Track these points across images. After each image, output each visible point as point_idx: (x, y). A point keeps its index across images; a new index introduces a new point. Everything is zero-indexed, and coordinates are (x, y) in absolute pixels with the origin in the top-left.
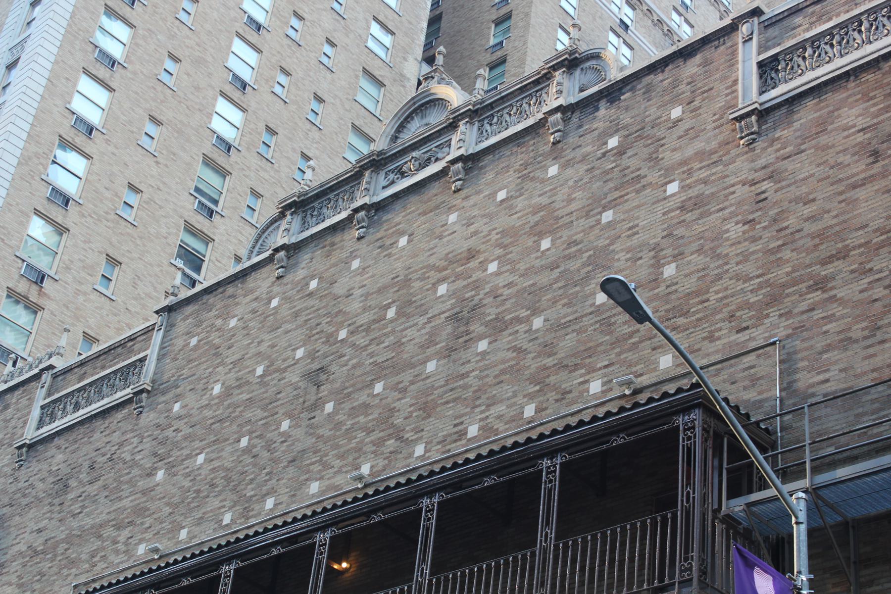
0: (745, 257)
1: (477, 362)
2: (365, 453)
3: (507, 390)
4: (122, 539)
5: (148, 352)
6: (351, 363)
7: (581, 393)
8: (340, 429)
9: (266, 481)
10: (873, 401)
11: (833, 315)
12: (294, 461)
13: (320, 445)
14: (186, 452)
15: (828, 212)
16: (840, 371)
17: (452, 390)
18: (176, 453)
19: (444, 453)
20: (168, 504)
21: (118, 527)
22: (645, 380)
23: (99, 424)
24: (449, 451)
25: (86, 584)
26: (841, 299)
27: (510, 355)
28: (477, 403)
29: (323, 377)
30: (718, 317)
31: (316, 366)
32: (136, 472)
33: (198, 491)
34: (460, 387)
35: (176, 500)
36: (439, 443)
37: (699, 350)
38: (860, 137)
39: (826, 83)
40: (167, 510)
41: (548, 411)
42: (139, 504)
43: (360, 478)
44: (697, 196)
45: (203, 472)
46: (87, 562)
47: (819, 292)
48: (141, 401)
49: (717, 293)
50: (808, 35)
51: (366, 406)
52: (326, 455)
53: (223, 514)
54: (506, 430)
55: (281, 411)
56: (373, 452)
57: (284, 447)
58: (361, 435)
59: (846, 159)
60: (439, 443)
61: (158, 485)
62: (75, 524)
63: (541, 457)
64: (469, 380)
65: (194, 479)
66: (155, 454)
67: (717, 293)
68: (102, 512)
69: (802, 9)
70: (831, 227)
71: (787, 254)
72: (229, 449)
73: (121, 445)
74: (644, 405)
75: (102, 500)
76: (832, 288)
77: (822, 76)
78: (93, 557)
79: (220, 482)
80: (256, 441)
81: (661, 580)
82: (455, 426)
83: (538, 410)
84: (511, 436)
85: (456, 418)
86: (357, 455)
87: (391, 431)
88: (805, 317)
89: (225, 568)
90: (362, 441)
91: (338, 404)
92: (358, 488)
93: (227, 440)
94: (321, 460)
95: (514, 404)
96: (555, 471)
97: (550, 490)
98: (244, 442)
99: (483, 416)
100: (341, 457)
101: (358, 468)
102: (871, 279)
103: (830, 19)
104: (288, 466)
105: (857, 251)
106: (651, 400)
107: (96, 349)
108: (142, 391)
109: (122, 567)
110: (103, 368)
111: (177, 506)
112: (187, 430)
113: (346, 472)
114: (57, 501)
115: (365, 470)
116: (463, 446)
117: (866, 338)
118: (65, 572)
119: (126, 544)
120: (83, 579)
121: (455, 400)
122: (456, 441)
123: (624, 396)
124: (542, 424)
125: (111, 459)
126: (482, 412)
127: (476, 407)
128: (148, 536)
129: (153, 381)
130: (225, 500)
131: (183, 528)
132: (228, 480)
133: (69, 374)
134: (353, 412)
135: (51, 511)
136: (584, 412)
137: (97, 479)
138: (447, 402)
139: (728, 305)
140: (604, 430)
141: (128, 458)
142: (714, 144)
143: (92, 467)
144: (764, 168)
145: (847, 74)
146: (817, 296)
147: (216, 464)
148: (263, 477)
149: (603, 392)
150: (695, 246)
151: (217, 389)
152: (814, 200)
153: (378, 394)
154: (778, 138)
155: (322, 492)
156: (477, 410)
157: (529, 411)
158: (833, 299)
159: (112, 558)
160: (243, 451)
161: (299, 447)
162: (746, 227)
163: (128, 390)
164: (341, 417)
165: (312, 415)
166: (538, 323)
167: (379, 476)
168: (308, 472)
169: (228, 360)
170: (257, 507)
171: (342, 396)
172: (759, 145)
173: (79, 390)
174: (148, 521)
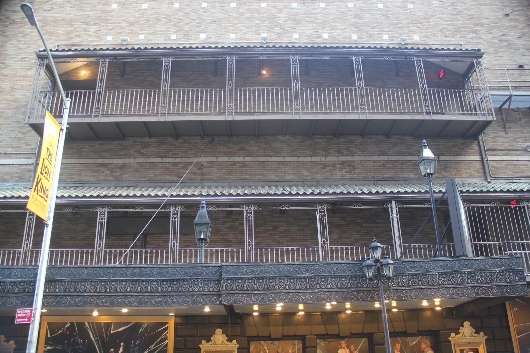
0: (443, 13)
1: (321, 10)
10: (501, 74)
15: (472, 9)
17: (309, 17)
22: (408, 41)
25: (66, 46)
27: (338, 13)
36: (306, 36)
49: (433, 21)
54: (343, 41)
56: (267, 30)
58: (257, 22)
62: (48, 15)
64: (319, 16)
67: (433, 21)
71: (459, 17)
76: (479, 34)
88: (471, 40)
98: (176, 6)
109: (94, 43)
117: (494, 54)
128: (113, 32)
139: (439, 26)
146: (473, 35)
152: (466, 3)
158: (480, 38)
159: (86, 37)
162: (441, 3)
164: (242, 10)
166: (350, 5)
170: (194, 36)
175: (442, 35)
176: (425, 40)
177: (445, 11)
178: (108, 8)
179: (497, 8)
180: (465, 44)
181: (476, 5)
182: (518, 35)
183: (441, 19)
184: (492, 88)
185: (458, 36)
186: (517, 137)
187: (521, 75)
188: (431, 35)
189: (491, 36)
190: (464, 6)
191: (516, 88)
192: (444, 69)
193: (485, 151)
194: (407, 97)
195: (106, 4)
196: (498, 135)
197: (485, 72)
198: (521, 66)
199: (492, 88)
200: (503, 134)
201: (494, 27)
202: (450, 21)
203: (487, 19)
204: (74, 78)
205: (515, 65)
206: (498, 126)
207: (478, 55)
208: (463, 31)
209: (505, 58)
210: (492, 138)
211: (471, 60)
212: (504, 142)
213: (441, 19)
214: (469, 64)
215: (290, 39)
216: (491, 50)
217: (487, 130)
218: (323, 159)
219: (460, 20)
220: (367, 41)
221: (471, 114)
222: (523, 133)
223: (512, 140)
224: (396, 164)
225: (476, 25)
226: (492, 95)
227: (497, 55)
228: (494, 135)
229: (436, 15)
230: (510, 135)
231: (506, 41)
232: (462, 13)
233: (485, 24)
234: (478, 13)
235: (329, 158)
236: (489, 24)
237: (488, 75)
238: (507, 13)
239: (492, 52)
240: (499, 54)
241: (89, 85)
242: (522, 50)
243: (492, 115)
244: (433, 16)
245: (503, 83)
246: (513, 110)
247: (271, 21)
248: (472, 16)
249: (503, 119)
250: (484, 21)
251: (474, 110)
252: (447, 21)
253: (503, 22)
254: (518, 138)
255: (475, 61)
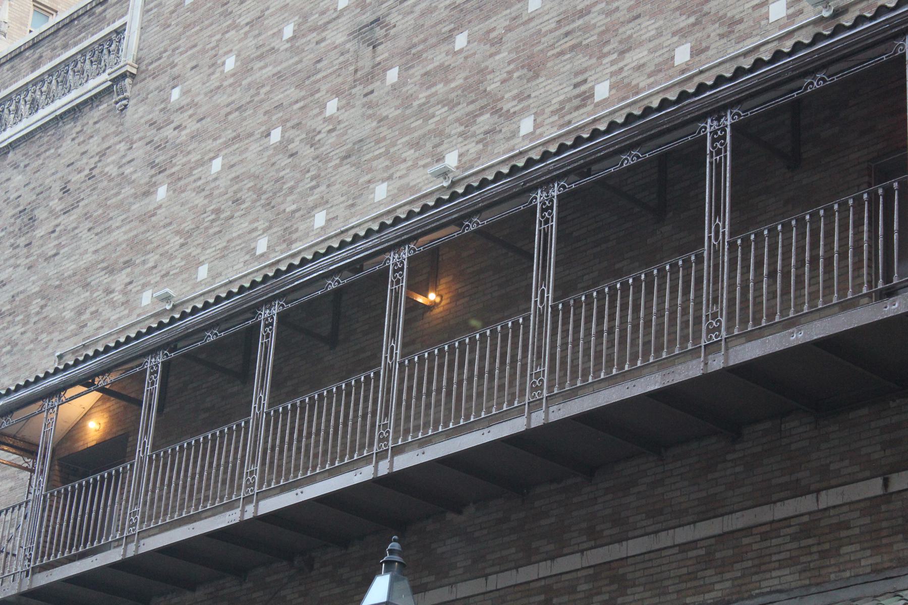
2: (450, 136)
3: (648, 27)
4: (118, 286)
5: (126, 19)
6: (418, 9)
7: (757, 22)
8: (410, 106)
9: (313, 188)
12: (346, 157)
13: (385, 131)
14: (194, 157)
17: (567, 34)
18: (180, 160)
19: (561, 126)
20: (178, 233)
21: (111, 270)
23: (71, 128)
24: (569, 122)
25: (74, 351)
28: (606, 50)
29: (379, 32)
31: (367, 17)
32: (128, 191)
33: (218, 211)
34: (579, 28)
35: (188, 225)
40: (177, 240)
41: (710, 53)
42: (136, 236)
43: (444, 174)
45: (223, 183)
46: (73, 320)
48: (123, 90)
51: (445, 69)
52: (394, 144)
53: (255, 239)
54: (650, 86)
55: (324, 88)
56: (461, 135)
57: (332, 139)
58: (441, 111)
60: (553, 113)
61: (160, 207)
62: (51, 271)
63: (703, 117)
65: (211, 194)
66: (152, 165)
68: (87, 248)
72: (255, 147)
73: (102, 154)
75: (85, 235)
78: (80, 314)
79: (248, 197)
80: (291, 133)
81: (888, 278)
82: (576, 86)
83: (696, 52)
84: (658, 92)
85: (577, 74)
86: (437, 140)
87: (483, 102)
89: (264, 314)
90: (443, 121)
91: (406, 68)
92: (443, 187)
93: (251, 135)
94: (387, 152)
95: (660, 47)
96: (724, 138)
97: (718, 166)
98: (276, 136)
99: (615, 68)
100: (416, 145)
101: (441, 159)
104: (341, 165)
106: (860, 19)
107: (54, 20)
108: (123, 76)
109: (121, 325)
110: (66, 47)
111: (189, 234)
112: (192, 126)
113: (425, 166)
114: (22, 241)
115: (451, 160)
116: (589, 115)
118: (44, 337)
119: (125, 293)
120: (69, 346)
121: (572, 48)
122: (577, 108)
123: (822, 19)
124: (701, 72)
125: (91, 177)
126: (613, 63)
127: (605, 55)
129: (138, 61)
130: (257, 220)
131: (202, 263)
132: (259, 192)
133: (17, 61)
134: (428, 79)
135: (16, 256)
136: (762, 49)
137: (74, 207)
138: (562, 53)
140: (793, 70)
141: (113, 170)
143: (65, 190)
147: (238, 170)
148: (307, 184)
149: (789, 17)
151: (230, 64)
153: (461, 51)
155: (393, 197)
156: (606, 60)
157: (682, 55)
159: (108, 313)
160: (275, 148)
161: (354, 135)
163: (104, 77)
164: (410, 88)
165: (370, 88)
167: (472, 167)
168: (370, 170)
169: (243, 21)
170: (302, 226)
171: (409, 57)
173: (34, 82)
174: (152, 259)
178: (148, 204)
194: (815, 245)
195: (146, 194)
204: (81, 446)
215: (512, 143)
218: (544, 569)
220: (724, 54)
224: (745, 541)
235: (564, 564)
241: (114, 450)
247: (472, 96)
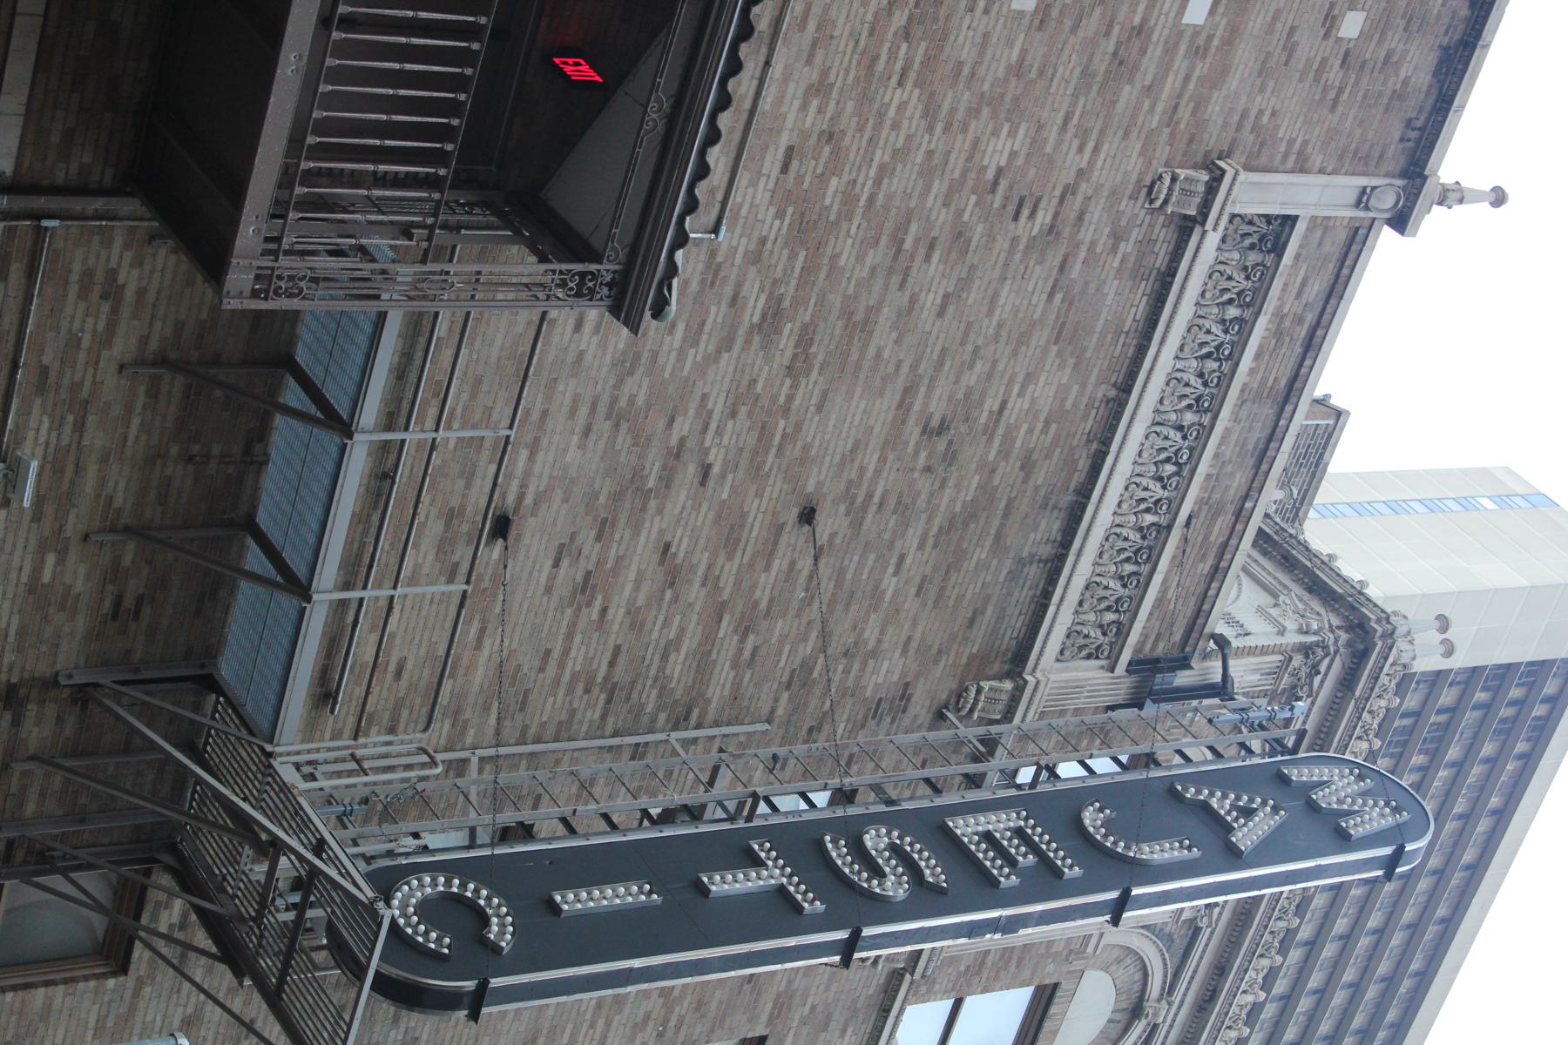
0: (928, 172)
10: (488, 411)
11: (695, 343)
16: (581, 354)
26: (716, 360)
30: (850, 105)
37: (809, 61)
38: (991, 404)
39: (1142, 350)
44: (1136, 67)
47: (756, 319)
49: (902, 107)
50: (1262, 323)
59: (970, 379)
67: (902, 107)
69: (1327, 302)
70: (866, 345)
74: (734, 48)
76: (748, 342)
77: (1159, 351)
88: (729, 290)
102: (716, 416)
103: (1258, 356)
105: (785, 391)
140: (694, 95)
142: (1215, 109)
144: (1080, 218)
145: (1126, 389)
146: (754, 307)
150: (1035, 59)
152: (941, 314)
154: (1115, 248)
158: (727, 344)
162: (990, 175)
172: (1135, 210)
175: (805, 135)
176: (802, 25)
177: (938, 187)
179: (862, 470)
180: (713, 253)
181: (914, 367)
182: (681, 548)
183: (899, 154)
184: (419, 330)
185: (773, 227)
186: (91, 419)
187: (451, 516)
188: (825, 73)
189: (718, 406)
190: (930, 301)
191: (382, 477)
192: (603, 93)
193: (38, 216)
196: (125, 313)
197: (525, 318)
198: (502, 527)
199: (419, 330)
200: (123, 346)
201: (764, 432)
202: (872, 198)
203: (820, 408)
205: (521, 497)
206: (179, 326)
207: (634, 294)
208: (793, 256)
209: (572, 455)
210: (112, 274)
211: (617, 250)
212: (74, 342)
213: (899, 154)
214: (596, 241)
216: (638, 387)
217: (167, 261)
219: (860, 259)
221: (286, 180)
222: (104, 460)
223: (76, 387)
225: (805, 339)
226: (382, 317)
227: (602, 409)
228: (129, 294)
229: (930, 129)
230: (112, 385)
231: (667, 481)
232: (896, 280)
233: (795, 386)
234: (866, 365)
236: (786, 410)
237: (502, 330)
238: (820, 518)
239: (629, 387)
240: (603, 427)
242: (591, 549)
243: (255, 294)
244: (930, 113)
245: (433, 412)
246: (261, 432)
248: (859, 326)
249: (216, 361)
250: (813, 384)
251: (306, 194)
252: (878, 183)
253: (776, 487)
254: (80, 427)
255: (606, 269)
